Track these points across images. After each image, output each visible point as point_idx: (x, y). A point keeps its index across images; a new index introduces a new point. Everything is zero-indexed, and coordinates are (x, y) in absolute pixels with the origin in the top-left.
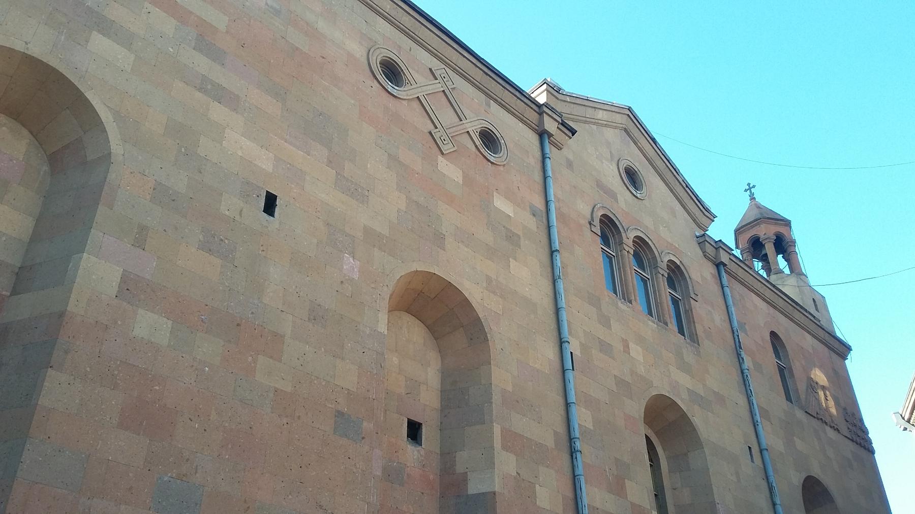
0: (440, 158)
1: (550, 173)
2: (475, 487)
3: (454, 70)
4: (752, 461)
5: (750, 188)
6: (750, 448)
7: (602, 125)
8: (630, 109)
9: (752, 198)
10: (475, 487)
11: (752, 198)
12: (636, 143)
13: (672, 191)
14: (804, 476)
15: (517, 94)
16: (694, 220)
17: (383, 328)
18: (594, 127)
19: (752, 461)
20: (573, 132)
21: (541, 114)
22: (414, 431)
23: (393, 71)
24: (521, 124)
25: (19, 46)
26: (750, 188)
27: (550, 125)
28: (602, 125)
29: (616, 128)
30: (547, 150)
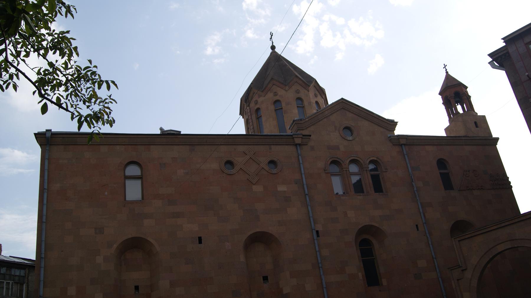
0: (253, 186)
1: (301, 162)
2: (285, 291)
3: (253, 145)
4: (418, 230)
5: (445, 66)
6: (417, 226)
7: (329, 116)
8: (342, 99)
9: (447, 72)
10: (285, 291)
11: (447, 72)
12: (349, 111)
13: (372, 122)
14: (452, 222)
15: (281, 137)
16: (387, 130)
17: (242, 258)
18: (325, 120)
19: (418, 230)
20: (310, 136)
21: (293, 138)
22: (265, 278)
23: (230, 163)
24: (286, 146)
25: (130, 237)
26: (445, 66)
27: (298, 141)
28: (329, 116)
29: (337, 111)
30: (299, 152)
